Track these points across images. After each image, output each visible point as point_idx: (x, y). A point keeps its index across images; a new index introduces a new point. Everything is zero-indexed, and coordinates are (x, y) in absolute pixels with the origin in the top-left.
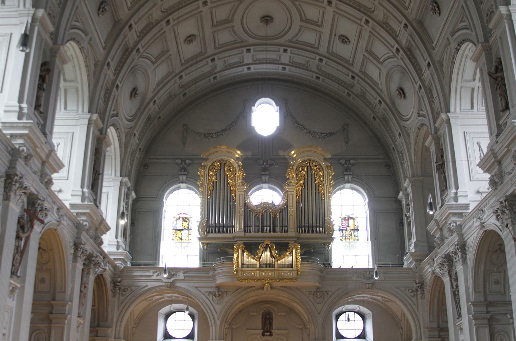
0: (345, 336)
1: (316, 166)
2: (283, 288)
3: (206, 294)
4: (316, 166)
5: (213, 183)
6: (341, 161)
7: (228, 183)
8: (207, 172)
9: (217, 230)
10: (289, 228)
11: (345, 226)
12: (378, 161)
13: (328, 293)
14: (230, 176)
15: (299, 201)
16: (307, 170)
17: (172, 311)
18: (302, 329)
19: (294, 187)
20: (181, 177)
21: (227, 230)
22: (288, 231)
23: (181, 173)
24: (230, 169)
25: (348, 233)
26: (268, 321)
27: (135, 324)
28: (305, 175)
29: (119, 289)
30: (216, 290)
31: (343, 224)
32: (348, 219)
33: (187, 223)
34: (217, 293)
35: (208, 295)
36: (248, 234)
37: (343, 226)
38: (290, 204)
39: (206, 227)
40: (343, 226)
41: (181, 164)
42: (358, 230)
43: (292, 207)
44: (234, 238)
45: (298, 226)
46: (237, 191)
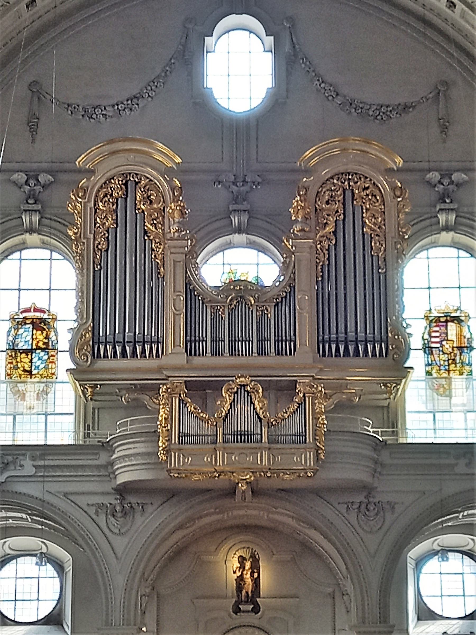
0: (439, 612)
1: (366, 188)
3: (92, 511)
4: (366, 188)
5: (108, 232)
6: (429, 176)
7: (145, 232)
9: (119, 349)
10: (298, 346)
11: (438, 340)
13: (393, 508)
14: (151, 216)
15: (322, 277)
20: (26, 219)
21: (143, 351)
22: (295, 350)
23: (27, 207)
24: (149, 197)
25: (445, 357)
30: (116, 499)
31: (433, 334)
32: (447, 321)
33: (44, 334)
34: (118, 508)
35: (97, 513)
36: (197, 360)
37: (433, 340)
39: (91, 343)
40: (433, 340)
41: (27, 183)
42: (471, 348)
44: (160, 369)
45: (321, 338)
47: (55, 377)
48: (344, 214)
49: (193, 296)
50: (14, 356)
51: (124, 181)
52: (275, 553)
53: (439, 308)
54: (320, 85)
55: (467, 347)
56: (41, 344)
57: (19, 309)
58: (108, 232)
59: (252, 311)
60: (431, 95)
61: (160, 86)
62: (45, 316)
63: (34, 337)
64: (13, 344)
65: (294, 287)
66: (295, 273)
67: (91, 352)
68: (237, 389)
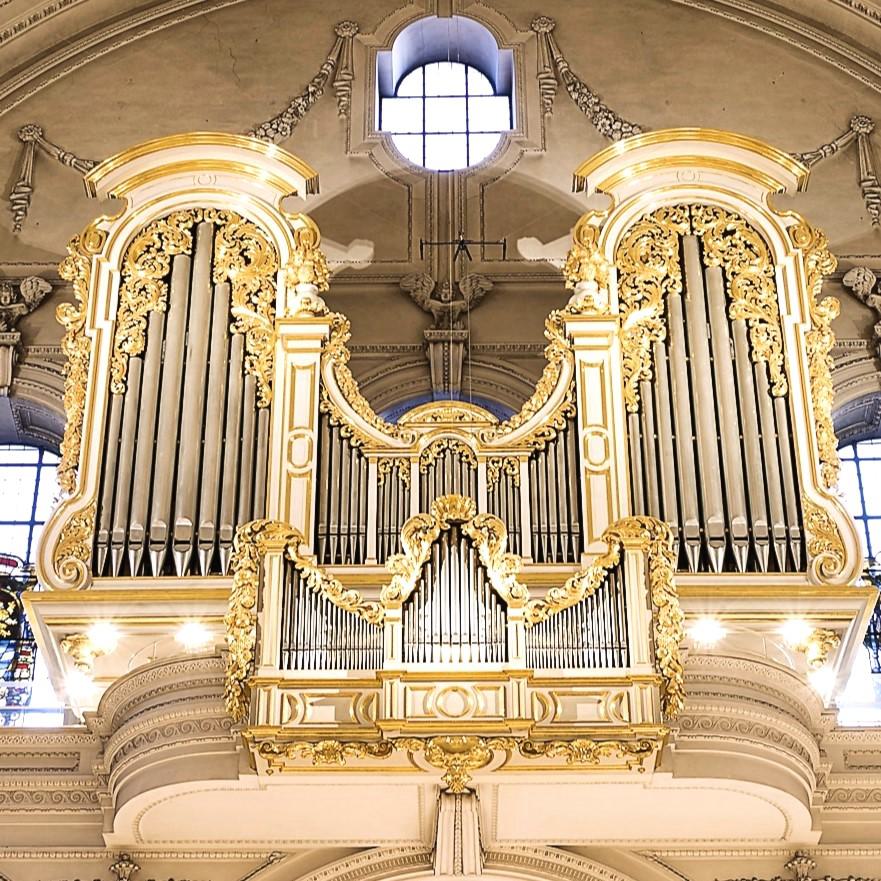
1: (732, 232)
7: (232, 319)
8: (112, 265)
15: (640, 403)
16: (681, 253)
19: (614, 326)
22: (581, 549)
28: (667, 277)
33: (11, 609)
38: (592, 412)
43: (605, 426)
46: (280, 355)
47: (24, 697)
48: (683, 281)
49: (336, 440)
54: (610, 125)
59: (476, 471)
60: (840, 143)
61: (284, 129)
62: (17, 572)
65: (575, 419)
66: (575, 389)
67: (89, 563)
68: (442, 532)
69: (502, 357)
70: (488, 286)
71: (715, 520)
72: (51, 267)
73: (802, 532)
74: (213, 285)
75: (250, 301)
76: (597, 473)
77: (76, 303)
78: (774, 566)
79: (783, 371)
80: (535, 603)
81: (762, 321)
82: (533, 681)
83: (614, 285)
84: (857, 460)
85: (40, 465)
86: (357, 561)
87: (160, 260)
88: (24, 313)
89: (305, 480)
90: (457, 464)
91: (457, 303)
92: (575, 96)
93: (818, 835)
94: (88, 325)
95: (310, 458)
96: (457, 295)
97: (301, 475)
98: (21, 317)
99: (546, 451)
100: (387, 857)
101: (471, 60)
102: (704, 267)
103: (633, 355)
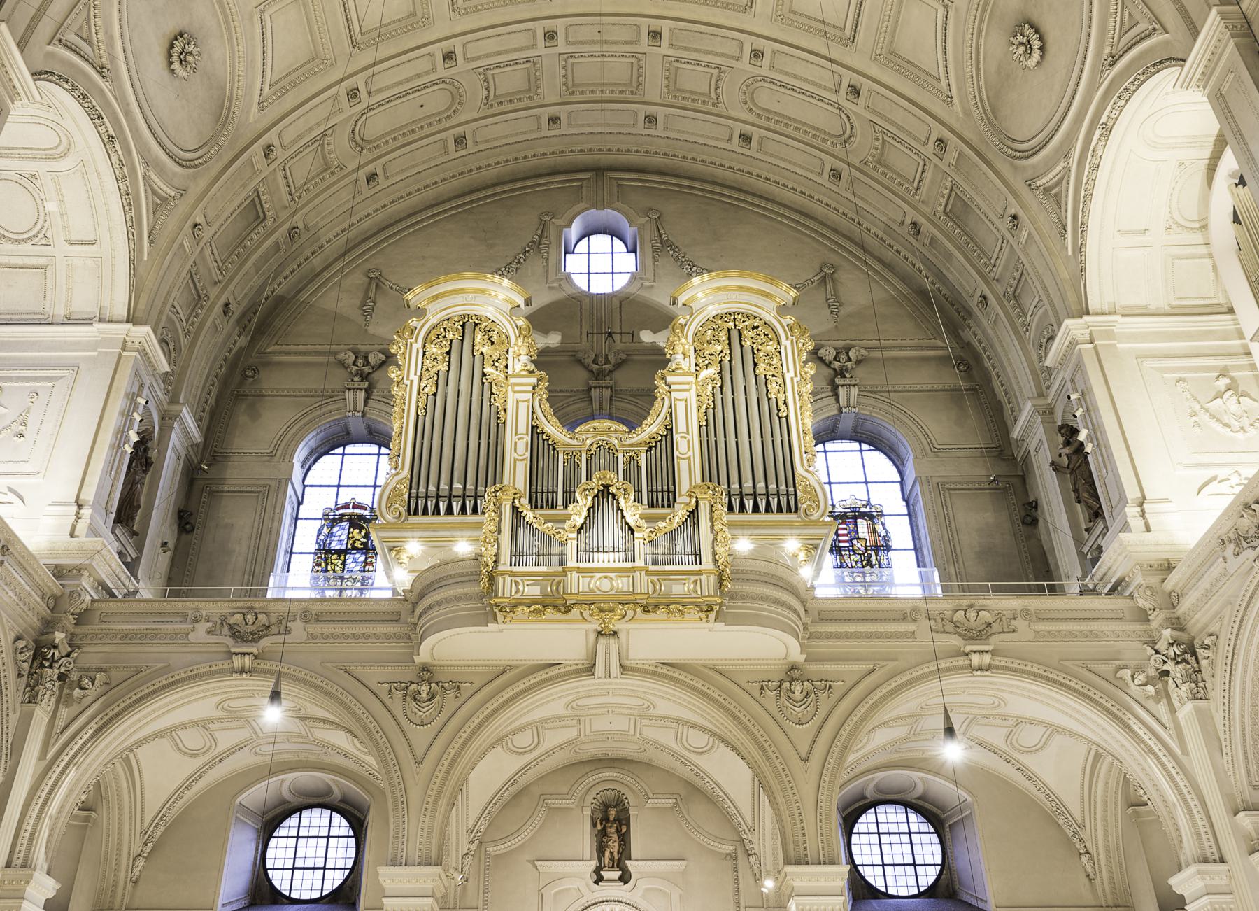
1: (757, 327)
2: (665, 670)
7: (484, 375)
8: (418, 345)
11: (846, 538)
12: (932, 353)
15: (707, 420)
16: (729, 339)
17: (285, 802)
18: (733, 857)
19: (692, 379)
22: (675, 500)
26: (613, 830)
27: (145, 844)
28: (722, 352)
29: (62, 677)
31: (840, 532)
32: (855, 518)
33: (363, 533)
38: (680, 426)
40: (840, 538)
41: (354, 364)
43: (688, 433)
46: (510, 394)
47: (370, 581)
48: (730, 354)
49: (541, 441)
50: (323, 556)
51: (461, 323)
52: (651, 796)
53: (844, 503)
55: (883, 546)
56: (357, 544)
57: (336, 505)
58: (437, 374)
59: (617, 457)
60: (816, 278)
61: (513, 271)
62: (366, 513)
63: (351, 535)
64: (324, 544)
65: (671, 429)
66: (671, 413)
67: (406, 508)
68: (599, 491)
69: (631, 396)
70: (624, 356)
71: (748, 484)
72: (385, 346)
73: (795, 491)
74: (474, 356)
75: (493, 365)
76: (683, 459)
77: (399, 366)
78: (780, 510)
79: (785, 403)
80: (649, 530)
81: (773, 376)
82: (648, 573)
83: (693, 356)
84: (825, 452)
85: (379, 454)
86: (552, 507)
87: (444, 342)
88: (371, 371)
89: (524, 462)
90: (607, 454)
91: (607, 366)
92: (671, 253)
93: (804, 657)
94: (405, 378)
95: (527, 451)
96: (607, 361)
97: (523, 460)
98: (369, 373)
99: (656, 447)
100: (568, 669)
101: (614, 233)
102: (742, 346)
103: (703, 394)
